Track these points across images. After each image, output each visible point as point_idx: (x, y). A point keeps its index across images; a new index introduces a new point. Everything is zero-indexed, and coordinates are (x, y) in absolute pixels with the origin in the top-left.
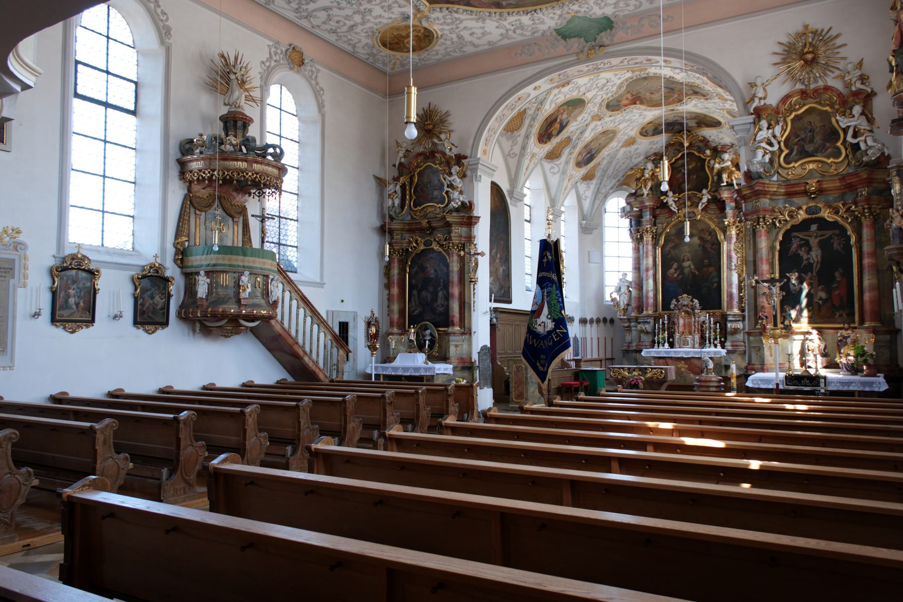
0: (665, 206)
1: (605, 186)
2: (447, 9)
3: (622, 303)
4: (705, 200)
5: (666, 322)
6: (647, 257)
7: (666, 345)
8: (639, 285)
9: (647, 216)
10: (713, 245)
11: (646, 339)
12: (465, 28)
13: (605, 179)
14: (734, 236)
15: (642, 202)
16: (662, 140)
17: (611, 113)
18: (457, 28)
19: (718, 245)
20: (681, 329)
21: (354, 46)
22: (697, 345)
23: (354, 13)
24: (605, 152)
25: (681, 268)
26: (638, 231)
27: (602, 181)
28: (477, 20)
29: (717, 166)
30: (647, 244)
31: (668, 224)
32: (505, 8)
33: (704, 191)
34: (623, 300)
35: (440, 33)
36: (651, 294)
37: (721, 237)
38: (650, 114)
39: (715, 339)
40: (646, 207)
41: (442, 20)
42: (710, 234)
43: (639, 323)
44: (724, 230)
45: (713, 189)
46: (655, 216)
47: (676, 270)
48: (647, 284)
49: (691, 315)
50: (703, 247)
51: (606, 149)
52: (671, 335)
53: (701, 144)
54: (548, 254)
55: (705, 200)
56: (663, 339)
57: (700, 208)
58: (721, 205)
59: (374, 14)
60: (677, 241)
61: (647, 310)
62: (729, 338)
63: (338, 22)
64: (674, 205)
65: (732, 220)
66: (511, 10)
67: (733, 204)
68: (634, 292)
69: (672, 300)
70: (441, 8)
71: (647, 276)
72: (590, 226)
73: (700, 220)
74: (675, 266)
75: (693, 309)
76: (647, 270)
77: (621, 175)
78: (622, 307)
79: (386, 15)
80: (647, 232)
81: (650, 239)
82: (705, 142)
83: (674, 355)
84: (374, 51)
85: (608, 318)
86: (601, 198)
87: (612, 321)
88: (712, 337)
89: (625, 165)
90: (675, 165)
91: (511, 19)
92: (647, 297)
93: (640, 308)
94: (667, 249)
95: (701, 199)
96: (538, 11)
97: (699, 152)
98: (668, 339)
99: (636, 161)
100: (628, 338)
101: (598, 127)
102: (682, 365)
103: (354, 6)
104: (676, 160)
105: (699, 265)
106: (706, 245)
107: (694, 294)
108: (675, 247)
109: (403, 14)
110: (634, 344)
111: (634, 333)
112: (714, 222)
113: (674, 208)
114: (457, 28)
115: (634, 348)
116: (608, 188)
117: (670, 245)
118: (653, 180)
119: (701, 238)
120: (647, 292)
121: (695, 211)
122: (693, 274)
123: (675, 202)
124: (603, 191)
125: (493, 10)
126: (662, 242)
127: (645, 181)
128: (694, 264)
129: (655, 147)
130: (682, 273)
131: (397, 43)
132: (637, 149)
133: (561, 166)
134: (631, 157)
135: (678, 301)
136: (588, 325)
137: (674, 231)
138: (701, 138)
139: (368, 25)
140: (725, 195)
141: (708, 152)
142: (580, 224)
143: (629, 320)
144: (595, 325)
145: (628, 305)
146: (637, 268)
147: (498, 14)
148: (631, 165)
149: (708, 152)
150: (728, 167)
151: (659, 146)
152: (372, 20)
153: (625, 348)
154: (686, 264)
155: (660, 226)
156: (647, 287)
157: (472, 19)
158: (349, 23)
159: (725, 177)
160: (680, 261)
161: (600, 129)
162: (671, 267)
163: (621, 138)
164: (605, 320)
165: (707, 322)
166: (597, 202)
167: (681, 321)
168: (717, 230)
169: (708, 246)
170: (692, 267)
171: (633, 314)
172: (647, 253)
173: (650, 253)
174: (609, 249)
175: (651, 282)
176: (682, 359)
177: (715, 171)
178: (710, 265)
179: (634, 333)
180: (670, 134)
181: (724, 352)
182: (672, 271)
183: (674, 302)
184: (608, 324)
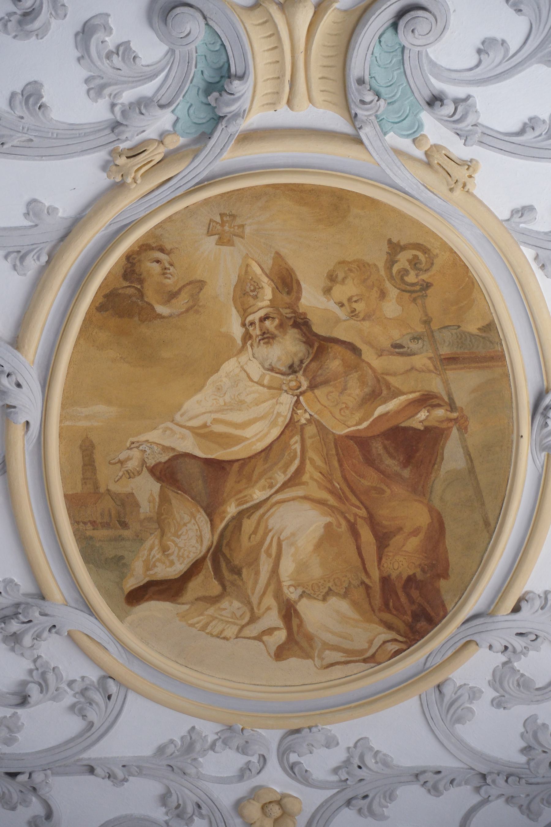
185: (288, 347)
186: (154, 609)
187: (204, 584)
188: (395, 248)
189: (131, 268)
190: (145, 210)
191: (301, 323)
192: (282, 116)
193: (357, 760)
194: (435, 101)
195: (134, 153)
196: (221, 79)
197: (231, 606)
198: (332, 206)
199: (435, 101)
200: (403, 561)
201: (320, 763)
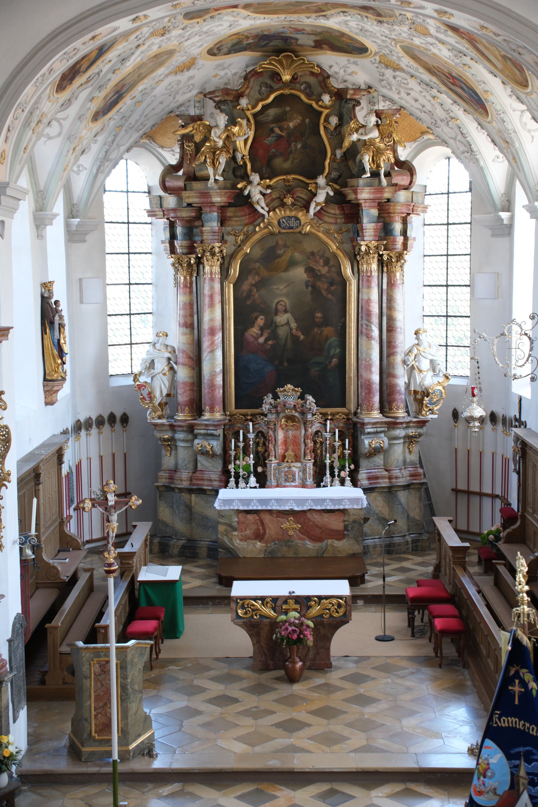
0: (242, 201)
1: (119, 146)
3: (157, 394)
4: (321, 197)
5: (251, 436)
6: (212, 305)
7: (253, 480)
8: (196, 361)
9: (212, 223)
10: (332, 284)
11: (212, 469)
13: (123, 132)
14: (375, 274)
15: (205, 194)
16: (238, 63)
17: (186, 22)
19: (343, 283)
20: (280, 450)
22: (310, 481)
24: (140, 87)
25: (271, 326)
26: (191, 250)
27: (115, 136)
29: (355, 137)
30: (212, 279)
31: (247, 237)
33: (321, 180)
34: (160, 387)
36: (219, 380)
37: (348, 271)
38: (247, 22)
39: (342, 468)
40: (212, 204)
42: (327, 262)
43: (195, 437)
44: (355, 257)
45: (334, 174)
46: (223, 222)
47: (262, 329)
48: (213, 359)
49: (293, 417)
50: (314, 287)
51: (145, 81)
52: (261, 459)
53: (312, 80)
54: (528, 677)
55: (321, 197)
56: (246, 468)
57: (312, 211)
58: (352, 213)
60: (264, 273)
61: (212, 410)
62: (364, 463)
64: (264, 205)
65: (374, 243)
67: (375, 212)
68: (183, 374)
69: (266, 395)
71: (213, 343)
72: (84, 226)
73: (307, 234)
74: (261, 321)
75: (303, 413)
76: (212, 332)
77: (149, 125)
78: (158, 399)
80: (213, 254)
81: (217, 269)
82: (323, 77)
83: (276, 507)
85: (118, 415)
86: (106, 163)
87: (125, 419)
88: (336, 464)
89: (161, 107)
90: (260, 118)
92: (212, 386)
93: (197, 407)
94: (246, 287)
95: (315, 195)
97: (308, 96)
98: (255, 466)
99: (181, 98)
100: (168, 461)
101: (155, 45)
102: (289, 524)
104: (265, 108)
105: (306, 321)
106: (318, 283)
107: (307, 387)
108: (261, 284)
110: (185, 475)
111: (183, 453)
112: (334, 240)
113: (262, 207)
115: (185, 484)
116: (123, 148)
117: (251, 280)
118: (228, 152)
119: (310, 270)
120: (213, 375)
121: (300, 215)
122: (295, 339)
123: (264, 195)
124: (113, 156)
126: (235, 271)
127: (214, 151)
128: (296, 321)
129: (222, 73)
130: (274, 335)
132: (192, 78)
133: (66, 124)
134: (177, 92)
135: (276, 397)
136: (83, 433)
137: (258, 252)
138: (316, 70)
140: (365, 195)
141: (326, 99)
142: (67, 225)
143: (172, 427)
144: (94, 431)
145: (168, 395)
146: (192, 323)
148: (173, 105)
149: (326, 99)
150: (372, 141)
151: (229, 73)
153: (163, 481)
154: (281, 319)
155: (230, 239)
156: (213, 365)
159: (367, 159)
160: (270, 313)
161: (155, 50)
162: (252, 325)
163: (178, 59)
164: (112, 418)
165: (328, 435)
166: (101, 177)
167: (281, 435)
168: (340, 254)
169: (323, 286)
170: (293, 325)
171: (180, 416)
172: (211, 297)
173: (218, 298)
174: (115, 268)
175: (219, 354)
176: (292, 512)
177: (346, 144)
178: (325, 323)
179: (183, 453)
180: (258, 54)
181: (358, 493)
182: (255, 330)
183: (269, 399)
184: (118, 425)
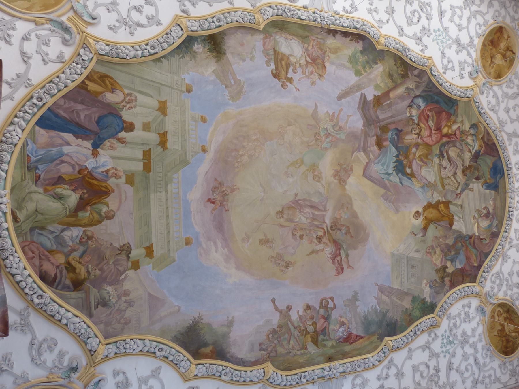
2: (484, 272)
12: (511, 274)
18: (507, 280)
21: (498, 380)
23: (463, 348)
28: (505, 260)
32: (500, 232)
35: (508, 298)
41: (496, 286)
59: (469, 333)
63: (467, 370)
66: (503, 229)
70: (482, 277)
79: (474, 324)
84: (510, 367)
91: (512, 234)
96: (511, 209)
103: (455, 342)
109: (477, 310)
114: (507, 280)
125: (498, 241)
131: (508, 341)
139: (479, 346)
147: (503, 240)
152: (476, 339)
157: (502, 264)
158: (471, 361)
185: (493, 60)
186: (514, 51)
187: (510, 49)
188: (483, 59)
189: (497, 78)
190: (493, 81)
191: (491, 61)
192: (482, 77)
193: (512, 22)
194: (474, 66)
195: (491, 86)
196: (484, 84)
197: (510, 45)
198: (484, 66)
199: (474, 66)
200: (498, 34)
201: (513, 24)
